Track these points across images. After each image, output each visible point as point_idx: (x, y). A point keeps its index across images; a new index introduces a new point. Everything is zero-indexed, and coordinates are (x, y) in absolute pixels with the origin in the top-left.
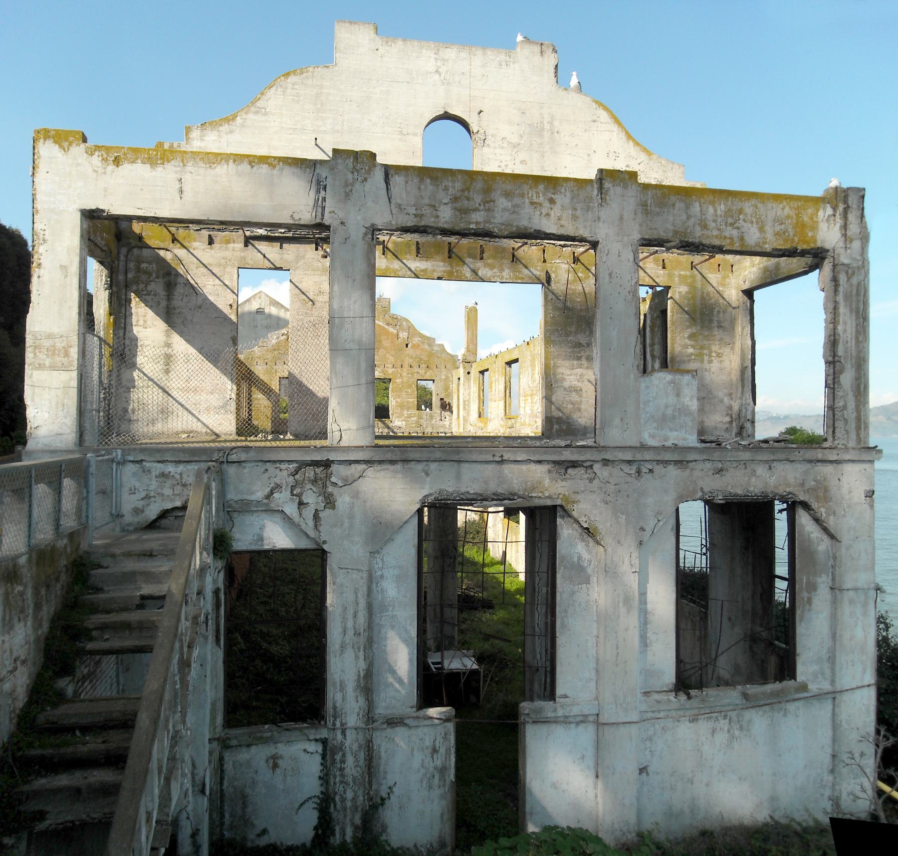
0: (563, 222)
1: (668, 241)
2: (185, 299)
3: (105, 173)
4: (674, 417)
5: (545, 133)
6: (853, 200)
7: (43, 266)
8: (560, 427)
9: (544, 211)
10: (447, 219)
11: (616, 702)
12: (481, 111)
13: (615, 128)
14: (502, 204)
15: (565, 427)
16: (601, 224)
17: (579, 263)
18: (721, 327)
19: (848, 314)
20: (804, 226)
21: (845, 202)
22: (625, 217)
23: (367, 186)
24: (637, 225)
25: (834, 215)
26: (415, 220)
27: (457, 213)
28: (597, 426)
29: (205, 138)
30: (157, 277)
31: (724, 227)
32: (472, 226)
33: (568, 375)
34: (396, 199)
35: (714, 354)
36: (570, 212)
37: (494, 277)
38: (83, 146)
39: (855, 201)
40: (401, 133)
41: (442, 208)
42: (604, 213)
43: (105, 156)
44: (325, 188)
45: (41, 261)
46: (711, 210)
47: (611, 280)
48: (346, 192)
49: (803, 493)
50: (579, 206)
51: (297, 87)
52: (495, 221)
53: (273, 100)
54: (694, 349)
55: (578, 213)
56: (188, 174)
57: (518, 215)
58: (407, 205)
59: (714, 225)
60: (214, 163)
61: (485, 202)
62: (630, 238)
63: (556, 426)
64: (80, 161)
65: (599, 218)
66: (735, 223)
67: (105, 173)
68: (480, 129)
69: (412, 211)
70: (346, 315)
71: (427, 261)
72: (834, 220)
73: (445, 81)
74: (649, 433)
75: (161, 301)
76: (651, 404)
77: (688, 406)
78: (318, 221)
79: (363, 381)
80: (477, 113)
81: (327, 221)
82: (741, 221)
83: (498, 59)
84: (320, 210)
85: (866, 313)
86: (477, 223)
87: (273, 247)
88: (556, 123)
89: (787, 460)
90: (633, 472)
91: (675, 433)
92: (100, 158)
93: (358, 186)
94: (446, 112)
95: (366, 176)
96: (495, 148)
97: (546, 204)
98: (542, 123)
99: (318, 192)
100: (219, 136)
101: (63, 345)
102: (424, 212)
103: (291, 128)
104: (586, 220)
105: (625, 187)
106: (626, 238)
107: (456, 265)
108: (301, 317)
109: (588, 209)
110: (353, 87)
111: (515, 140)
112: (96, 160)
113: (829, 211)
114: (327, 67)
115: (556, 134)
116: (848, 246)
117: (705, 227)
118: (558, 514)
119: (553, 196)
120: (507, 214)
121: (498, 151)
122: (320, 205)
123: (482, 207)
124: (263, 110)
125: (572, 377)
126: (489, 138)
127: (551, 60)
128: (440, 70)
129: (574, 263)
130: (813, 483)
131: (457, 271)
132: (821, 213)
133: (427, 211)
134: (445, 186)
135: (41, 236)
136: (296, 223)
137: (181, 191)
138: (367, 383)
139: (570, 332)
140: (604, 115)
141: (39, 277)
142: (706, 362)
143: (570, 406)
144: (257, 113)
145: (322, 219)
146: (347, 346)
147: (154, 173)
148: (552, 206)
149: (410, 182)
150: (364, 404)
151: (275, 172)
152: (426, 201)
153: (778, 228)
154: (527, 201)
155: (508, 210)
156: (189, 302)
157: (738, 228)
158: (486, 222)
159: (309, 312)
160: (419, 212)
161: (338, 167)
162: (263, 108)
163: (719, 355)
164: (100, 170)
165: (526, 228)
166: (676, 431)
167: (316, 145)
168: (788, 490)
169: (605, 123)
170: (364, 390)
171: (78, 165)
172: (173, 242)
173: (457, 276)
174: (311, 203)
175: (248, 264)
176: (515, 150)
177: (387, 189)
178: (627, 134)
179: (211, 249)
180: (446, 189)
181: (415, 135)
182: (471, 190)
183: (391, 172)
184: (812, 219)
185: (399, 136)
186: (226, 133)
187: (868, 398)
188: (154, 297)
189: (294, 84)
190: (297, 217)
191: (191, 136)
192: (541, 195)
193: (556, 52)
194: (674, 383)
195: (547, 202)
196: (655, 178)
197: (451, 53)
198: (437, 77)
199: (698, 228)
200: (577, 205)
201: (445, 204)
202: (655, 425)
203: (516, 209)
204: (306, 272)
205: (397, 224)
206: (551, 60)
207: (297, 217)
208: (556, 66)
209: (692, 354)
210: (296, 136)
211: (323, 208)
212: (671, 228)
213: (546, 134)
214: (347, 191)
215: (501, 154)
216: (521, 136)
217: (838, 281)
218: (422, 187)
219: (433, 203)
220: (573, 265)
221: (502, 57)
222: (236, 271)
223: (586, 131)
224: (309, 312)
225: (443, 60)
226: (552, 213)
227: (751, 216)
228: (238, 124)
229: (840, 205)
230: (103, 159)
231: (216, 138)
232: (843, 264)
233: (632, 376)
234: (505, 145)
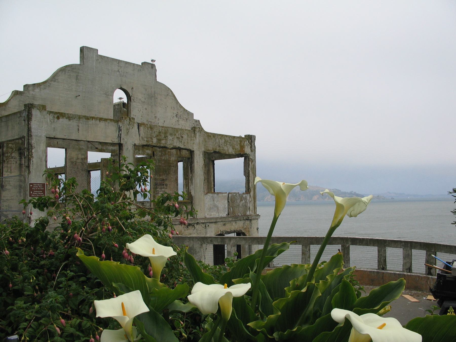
0: (185, 144)
9: (180, 140)
16: (194, 145)
32: (162, 145)
33: (160, 191)
34: (141, 135)
36: (187, 141)
44: (121, 131)
46: (221, 141)
51: (70, 72)
61: (165, 137)
65: (194, 143)
66: (226, 145)
68: (132, 95)
69: (146, 139)
71: (115, 146)
78: (119, 142)
81: (122, 142)
82: (228, 145)
86: (163, 144)
88: (156, 95)
90: (204, 226)
94: (121, 87)
97: (181, 138)
98: (152, 94)
99: (119, 132)
102: (149, 140)
109: (191, 140)
111: (143, 100)
115: (156, 99)
117: (219, 146)
122: (120, 137)
128: (119, 70)
130: (245, 227)
133: (150, 139)
145: (121, 141)
152: (149, 136)
157: (227, 147)
158: (166, 143)
165: (176, 146)
168: (240, 229)
169: (171, 96)
198: (118, 73)
199: (218, 147)
201: (155, 137)
202: (208, 211)
217: (249, 164)
218: (148, 131)
219: (151, 137)
232: (251, 159)
233: (203, 195)
234: (140, 102)
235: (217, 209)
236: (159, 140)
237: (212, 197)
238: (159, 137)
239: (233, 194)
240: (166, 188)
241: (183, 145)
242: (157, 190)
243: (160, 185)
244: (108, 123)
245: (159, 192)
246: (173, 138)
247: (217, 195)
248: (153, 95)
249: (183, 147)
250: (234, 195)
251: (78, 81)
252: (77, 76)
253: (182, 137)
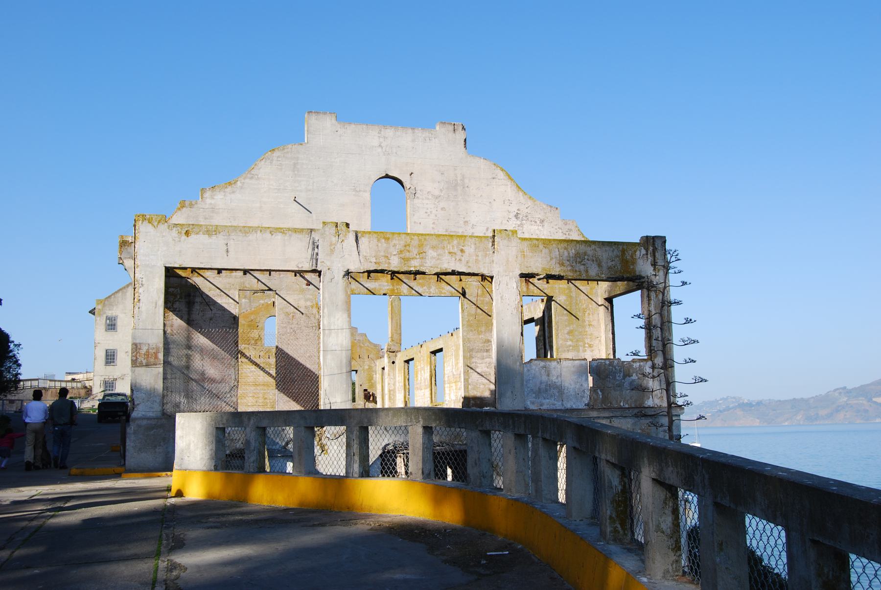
0: (470, 264)
1: (538, 275)
2: (201, 314)
3: (180, 241)
4: (546, 390)
5: (458, 188)
6: (658, 244)
7: (141, 301)
8: (475, 402)
10: (396, 265)
12: (412, 173)
13: (509, 183)
14: (431, 254)
15: (479, 402)
16: (494, 265)
17: (486, 281)
18: (591, 325)
20: (627, 262)
21: (654, 244)
22: (510, 260)
23: (344, 244)
24: (518, 265)
25: (647, 254)
26: (375, 266)
27: (402, 261)
28: (497, 397)
29: (215, 197)
30: (181, 298)
31: (574, 264)
33: (480, 364)
35: (587, 345)
36: (475, 258)
37: (424, 293)
38: (166, 224)
39: (660, 245)
40: (355, 190)
41: (393, 257)
42: (496, 257)
43: (180, 230)
44: (318, 247)
45: (140, 298)
47: (502, 301)
48: (331, 249)
50: (480, 254)
52: (427, 265)
53: (265, 169)
54: (572, 342)
55: (480, 258)
56: (232, 240)
57: (441, 261)
58: (370, 256)
60: (248, 233)
62: (514, 273)
64: (164, 234)
65: (493, 261)
66: (582, 261)
67: (180, 241)
68: (412, 186)
69: (374, 260)
70: (332, 328)
71: (375, 282)
72: (647, 257)
73: (386, 153)
74: (531, 401)
75: (183, 315)
76: (531, 382)
77: (555, 382)
78: (314, 268)
79: (344, 370)
80: (409, 175)
83: (424, 135)
84: (315, 261)
85: (669, 317)
87: (264, 274)
88: (466, 181)
89: (622, 416)
91: (548, 401)
92: (177, 232)
93: (339, 245)
94: (387, 175)
95: (343, 238)
96: (423, 199)
97: (459, 253)
98: (456, 180)
99: (314, 249)
100: (225, 195)
101: (154, 351)
102: (381, 261)
103: (276, 189)
104: (484, 263)
105: (509, 239)
106: (511, 274)
107: (396, 285)
108: (285, 325)
109: (486, 255)
110: (320, 158)
111: (437, 193)
112: (174, 233)
113: (643, 252)
114: (301, 144)
116: (657, 274)
119: (463, 248)
120: (434, 260)
121: (425, 201)
122: (315, 258)
123: (418, 256)
124: (256, 176)
125: (483, 365)
126: (418, 192)
127: (461, 136)
128: (382, 145)
129: (482, 281)
131: (397, 289)
132: (638, 253)
133: (383, 260)
134: (394, 244)
135: (140, 282)
136: (300, 269)
137: (227, 251)
138: (347, 372)
139: (481, 331)
140: (501, 175)
141: (139, 308)
142: (581, 351)
143: (482, 386)
144: (252, 178)
145: (316, 267)
146: (333, 348)
147: (210, 240)
148: (463, 254)
149: (372, 242)
150: (345, 386)
151: (286, 238)
152: (382, 254)
153: (610, 264)
154: (447, 251)
155: (435, 258)
156: (203, 316)
157: (584, 265)
158: (421, 266)
159: (291, 321)
160: (378, 261)
161: (326, 233)
162: (256, 175)
163: (590, 346)
164: (177, 239)
166: (548, 399)
167: (295, 200)
170: (345, 377)
171: (163, 236)
172: (192, 273)
173: (398, 292)
174: (309, 257)
175: (246, 287)
176: (437, 201)
177: (357, 247)
178: (518, 187)
179: (220, 277)
180: (395, 245)
181: (365, 191)
182: (411, 246)
183: (359, 235)
184: (632, 257)
185: (354, 193)
186: (230, 193)
187: (674, 373)
188: (178, 313)
189: (278, 157)
190: (300, 266)
191: (205, 196)
192: (455, 247)
193: (465, 129)
194: (546, 368)
195: (459, 252)
196: (539, 218)
197: (389, 132)
198: (380, 150)
200: (479, 253)
202: (534, 395)
203: (440, 257)
204: (288, 293)
205: (364, 269)
206: (461, 136)
207: (300, 266)
208: (465, 140)
209: (570, 346)
210: (279, 194)
211: (317, 260)
212: (540, 266)
213: (459, 188)
214: (332, 248)
215: (427, 204)
216: (441, 190)
217: (651, 297)
218: (380, 244)
220: (482, 283)
221: (426, 134)
222: (238, 293)
223: (488, 185)
224: (291, 321)
225: (384, 137)
226: (463, 259)
227: (592, 256)
228: (238, 187)
229: (650, 247)
230: (179, 232)
231: (222, 197)
234: (430, 197)
235: (558, 392)
236: (406, 260)
238: (404, 255)
239: (603, 361)
242: (473, 360)
243: (480, 352)
244: (290, 236)
245: (478, 365)
246: (438, 255)
247: (558, 362)
248: (459, 182)
250: (605, 364)
251: (296, 172)
252: (295, 165)
253: (462, 251)
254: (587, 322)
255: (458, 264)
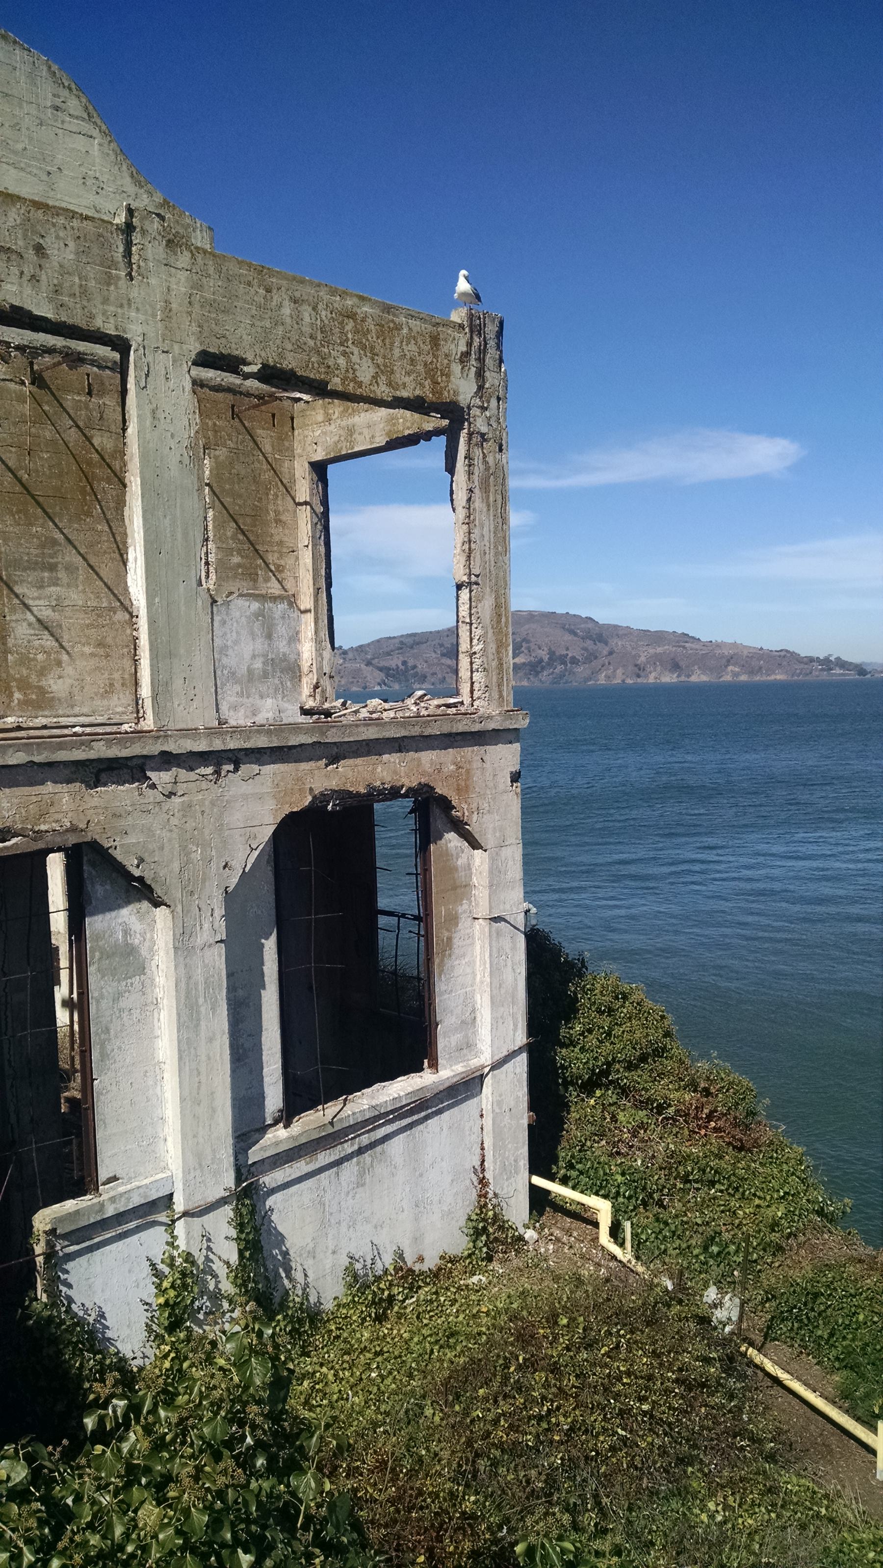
9: (28, 270)
11: (200, 1165)
19: (485, 510)
49: (440, 783)
59: (311, 343)
62: (184, 347)
63: (17, 695)
97: (30, 254)
118: (85, 859)
142: (261, 579)
169: (77, 118)
237: (259, 614)
240: (69, 585)
241: (50, 300)
243: (34, 569)
249: (49, 316)
254: (272, 514)
255: (28, 290)
